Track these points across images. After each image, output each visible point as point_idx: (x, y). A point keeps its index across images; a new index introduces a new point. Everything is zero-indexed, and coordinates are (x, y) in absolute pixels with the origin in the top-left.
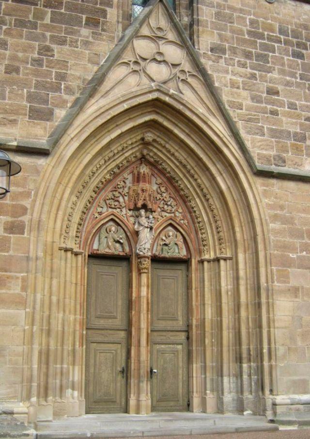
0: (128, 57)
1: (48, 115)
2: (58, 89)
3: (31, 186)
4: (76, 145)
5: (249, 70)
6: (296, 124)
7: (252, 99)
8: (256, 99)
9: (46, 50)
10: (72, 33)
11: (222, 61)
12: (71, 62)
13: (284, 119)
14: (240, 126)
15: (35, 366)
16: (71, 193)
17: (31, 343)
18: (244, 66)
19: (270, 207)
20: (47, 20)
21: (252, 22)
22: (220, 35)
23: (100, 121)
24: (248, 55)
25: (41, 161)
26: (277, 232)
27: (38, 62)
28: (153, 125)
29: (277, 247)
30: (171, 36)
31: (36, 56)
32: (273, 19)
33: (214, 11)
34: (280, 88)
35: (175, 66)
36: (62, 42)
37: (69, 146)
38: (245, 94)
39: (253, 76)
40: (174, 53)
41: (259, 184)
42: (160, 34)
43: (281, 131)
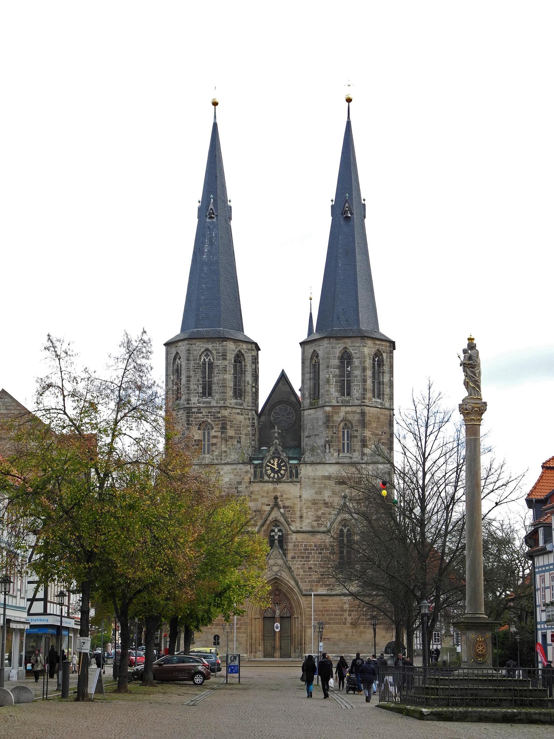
8: (305, 572)
14: (299, 580)
17: (247, 642)
18: (301, 561)
21: (305, 545)
24: (303, 557)
30: (280, 557)
33: (293, 544)
34: (313, 566)
35: (280, 566)
38: (301, 571)
39: (304, 564)
40: (280, 562)
41: (304, 598)
42: (276, 557)
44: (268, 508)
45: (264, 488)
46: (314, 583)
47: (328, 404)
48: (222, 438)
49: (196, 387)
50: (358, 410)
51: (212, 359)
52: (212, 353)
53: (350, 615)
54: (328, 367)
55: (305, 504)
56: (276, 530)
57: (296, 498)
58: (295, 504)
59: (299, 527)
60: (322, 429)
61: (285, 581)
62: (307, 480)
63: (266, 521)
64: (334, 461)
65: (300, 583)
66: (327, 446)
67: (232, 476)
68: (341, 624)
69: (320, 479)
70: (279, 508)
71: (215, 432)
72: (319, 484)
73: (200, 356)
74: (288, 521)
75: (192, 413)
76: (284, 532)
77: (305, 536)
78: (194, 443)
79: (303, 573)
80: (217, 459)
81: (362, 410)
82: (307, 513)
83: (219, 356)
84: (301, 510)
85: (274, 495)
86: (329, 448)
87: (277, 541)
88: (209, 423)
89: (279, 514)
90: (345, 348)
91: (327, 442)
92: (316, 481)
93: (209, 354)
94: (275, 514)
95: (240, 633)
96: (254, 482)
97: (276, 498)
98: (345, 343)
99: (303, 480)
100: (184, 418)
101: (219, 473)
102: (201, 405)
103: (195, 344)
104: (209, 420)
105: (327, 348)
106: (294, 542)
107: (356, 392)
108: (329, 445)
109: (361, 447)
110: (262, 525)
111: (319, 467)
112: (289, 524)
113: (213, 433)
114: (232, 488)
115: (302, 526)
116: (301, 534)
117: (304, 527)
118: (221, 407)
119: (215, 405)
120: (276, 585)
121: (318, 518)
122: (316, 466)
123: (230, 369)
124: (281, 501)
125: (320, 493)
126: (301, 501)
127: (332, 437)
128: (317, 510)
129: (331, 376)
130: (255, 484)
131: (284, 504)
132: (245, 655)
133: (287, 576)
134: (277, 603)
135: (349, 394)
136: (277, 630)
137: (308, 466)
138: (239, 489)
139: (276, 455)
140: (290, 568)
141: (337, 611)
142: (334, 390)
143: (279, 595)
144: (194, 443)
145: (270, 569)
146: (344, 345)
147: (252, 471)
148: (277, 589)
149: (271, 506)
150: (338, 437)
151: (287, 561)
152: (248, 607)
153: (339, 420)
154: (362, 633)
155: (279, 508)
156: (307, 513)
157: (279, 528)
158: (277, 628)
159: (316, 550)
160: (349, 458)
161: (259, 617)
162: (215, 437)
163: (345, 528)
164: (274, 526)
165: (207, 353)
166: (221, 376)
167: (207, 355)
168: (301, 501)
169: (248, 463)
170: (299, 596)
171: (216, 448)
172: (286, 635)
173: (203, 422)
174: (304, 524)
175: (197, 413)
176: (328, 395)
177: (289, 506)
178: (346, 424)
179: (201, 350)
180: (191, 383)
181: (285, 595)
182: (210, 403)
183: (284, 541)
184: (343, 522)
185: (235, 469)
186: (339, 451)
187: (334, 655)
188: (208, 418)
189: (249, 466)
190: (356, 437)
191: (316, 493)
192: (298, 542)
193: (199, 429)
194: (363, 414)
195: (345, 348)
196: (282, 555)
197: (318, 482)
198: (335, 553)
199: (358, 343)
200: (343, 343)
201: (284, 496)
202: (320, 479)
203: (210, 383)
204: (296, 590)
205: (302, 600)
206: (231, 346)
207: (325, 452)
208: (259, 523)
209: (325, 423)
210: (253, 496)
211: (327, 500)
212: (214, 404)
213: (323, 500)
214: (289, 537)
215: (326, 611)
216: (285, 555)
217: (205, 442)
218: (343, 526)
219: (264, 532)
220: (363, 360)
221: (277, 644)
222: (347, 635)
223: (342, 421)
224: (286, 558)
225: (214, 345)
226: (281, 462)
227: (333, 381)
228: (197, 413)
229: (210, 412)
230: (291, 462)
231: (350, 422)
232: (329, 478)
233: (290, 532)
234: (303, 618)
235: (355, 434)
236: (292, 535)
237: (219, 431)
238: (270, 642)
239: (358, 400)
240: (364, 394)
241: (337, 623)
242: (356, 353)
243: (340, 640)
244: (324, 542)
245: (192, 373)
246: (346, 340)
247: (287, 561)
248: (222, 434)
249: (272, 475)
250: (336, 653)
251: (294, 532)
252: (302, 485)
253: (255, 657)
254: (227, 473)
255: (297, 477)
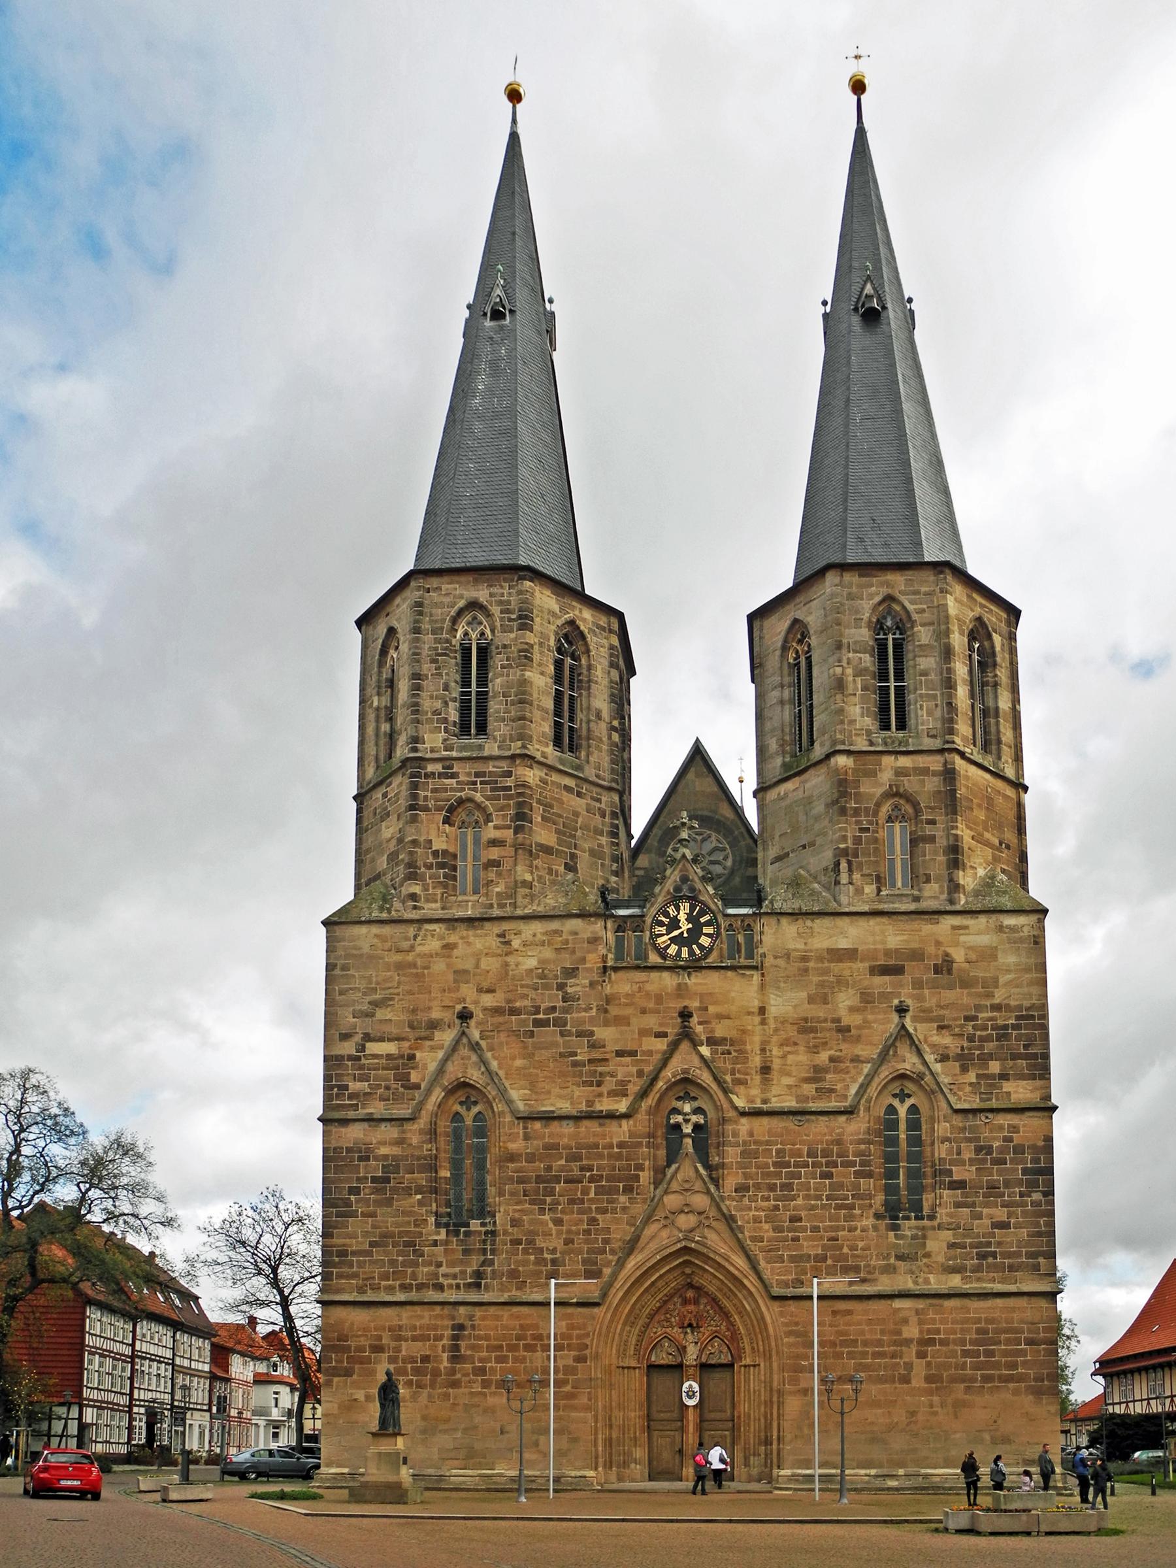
0: (660, 1214)
1: (597, 1274)
2: (604, 1252)
3: (590, 1329)
4: (621, 1294)
5: (772, 1202)
6: (818, 1245)
7: (774, 1230)
9: (593, 1221)
10: (612, 1202)
11: (746, 1201)
12: (613, 1227)
13: (805, 1243)
14: (761, 1256)
15: (600, 1449)
16: (625, 1324)
17: (596, 1434)
18: (768, 1199)
19: (786, 1325)
20: (592, 1195)
21: (778, 1152)
22: (744, 1173)
23: (639, 1273)
24: (772, 1188)
25: (596, 1310)
26: (790, 1345)
27: (587, 1232)
28: (687, 1263)
29: (789, 1358)
30: (698, 1185)
31: (586, 1227)
32: (802, 1142)
33: (739, 1150)
34: (803, 1214)
35: (700, 1213)
36: (604, 1211)
37: (616, 1295)
38: (766, 1226)
39: (776, 1208)
40: (700, 1201)
41: (776, 1307)
42: (687, 1186)
43: (801, 1256)
44: (661, 1045)
45: (649, 987)
46: (808, 1261)
47: (842, 747)
48: (517, 847)
49: (438, 704)
50: (935, 763)
51: (488, 632)
52: (489, 615)
53: (921, 1355)
54: (839, 646)
55: (776, 1030)
56: (687, 1108)
57: (749, 1013)
58: (744, 1032)
59: (758, 1101)
60: (826, 822)
61: (718, 1258)
62: (781, 962)
63: (654, 1080)
64: (866, 908)
65: (762, 1263)
66: (844, 865)
67: (548, 953)
68: (894, 1382)
69: (821, 959)
70: (695, 1044)
71: (496, 827)
72: (822, 975)
73: (454, 621)
74: (725, 1082)
75: (427, 776)
76: (711, 1114)
77: (776, 1123)
78: (431, 860)
79: (771, 1234)
80: (502, 906)
81: (946, 763)
82: (784, 1057)
83: (510, 620)
84: (763, 1050)
85: (679, 1005)
86: (850, 870)
87: (689, 1141)
88: (478, 806)
89: (696, 1061)
90: (889, 598)
91: (845, 852)
92: (811, 964)
93: (481, 617)
94: (683, 1062)
95: (574, 1408)
96: (615, 969)
97: (685, 1015)
98: (888, 584)
99: (769, 960)
100: (405, 793)
101: (508, 943)
102: (454, 754)
103: (440, 589)
104: (478, 797)
105: (833, 595)
106: (745, 1143)
107: (924, 716)
108: (849, 863)
109: (948, 868)
110: (644, 1094)
111: (820, 924)
112: (726, 1091)
113: (490, 832)
114: (546, 987)
115: (768, 1095)
116: (765, 1121)
117: (774, 1100)
118: (513, 757)
119: (496, 752)
120: (688, 1271)
121: (817, 1074)
122: (809, 923)
123: (545, 660)
124: (700, 1023)
125: (825, 1001)
126: (763, 1022)
127: (857, 840)
128: (814, 1050)
129: (849, 671)
130: (621, 974)
131: (712, 1031)
132: (592, 1473)
133: (722, 1245)
134: (690, 1325)
135: (902, 725)
136: (691, 1403)
137: (784, 921)
138: (569, 990)
139: (685, 891)
140: (729, 1220)
141: (879, 1343)
142: (858, 709)
143: (696, 1302)
144: (431, 860)
145: (669, 1220)
146: (884, 591)
147: (611, 937)
148: (690, 1286)
149: (670, 1038)
150: (876, 840)
151: (722, 1198)
152: (600, 1334)
153: (879, 791)
154: (959, 1405)
155: (695, 1044)
156: (784, 1057)
157: (696, 1104)
158: (690, 1397)
159: (814, 1165)
160: (910, 899)
161: (634, 1364)
162: (494, 843)
163: (902, 1101)
164: (679, 1099)
165: (475, 618)
166: (515, 675)
167: (474, 621)
168: (763, 1022)
169: (596, 915)
170: (760, 1301)
171: (499, 874)
172: (718, 1415)
173: (461, 802)
174: (775, 1090)
175: (441, 775)
176: (842, 722)
177: (725, 1039)
178: (896, 807)
179: (455, 604)
180: (424, 694)
181: (715, 1301)
182: (481, 747)
183: (713, 1140)
184: (897, 1083)
185: (556, 932)
186: (879, 879)
187: (873, 1472)
188: (475, 790)
189: (600, 924)
190: (932, 839)
191: (811, 1000)
192: (755, 1142)
193: (447, 821)
194: (949, 774)
195: (889, 598)
196: (707, 1179)
197: (817, 969)
198: (870, 1175)
199: (926, 582)
200: (882, 584)
201: (712, 1009)
202: (821, 959)
203: (483, 697)
204: (751, 1282)
205: (771, 1313)
206: (544, 599)
207: (837, 883)
208: (633, 1089)
209: (837, 801)
210: (614, 1011)
211: (846, 1020)
212: (491, 748)
213: (834, 1021)
214: (729, 1128)
215: (844, 1343)
216: (716, 1182)
217: (464, 859)
218: (895, 1096)
219: (649, 1113)
220: (943, 627)
221: (691, 1441)
222: (913, 1414)
223: (888, 795)
224: (717, 1186)
225: (495, 590)
226: (702, 913)
227: (855, 684)
228: (441, 775)
229: (483, 774)
230: (730, 911)
231: (909, 798)
232: (851, 954)
233: (732, 1114)
234: (775, 1365)
235: (929, 830)
236: (736, 1122)
237: (509, 827)
238: (668, 1436)
239: (934, 736)
240: (951, 721)
241: (881, 1380)
242: (923, 611)
243: (891, 1427)
244: (839, 1142)
245: (427, 668)
246: (891, 577)
247: (722, 1198)
248: (516, 833)
249: (672, 950)
250: (880, 1466)
251: (743, 1114)
252: (767, 978)
253: (620, 1479)
254: (533, 944)
255: (750, 956)
